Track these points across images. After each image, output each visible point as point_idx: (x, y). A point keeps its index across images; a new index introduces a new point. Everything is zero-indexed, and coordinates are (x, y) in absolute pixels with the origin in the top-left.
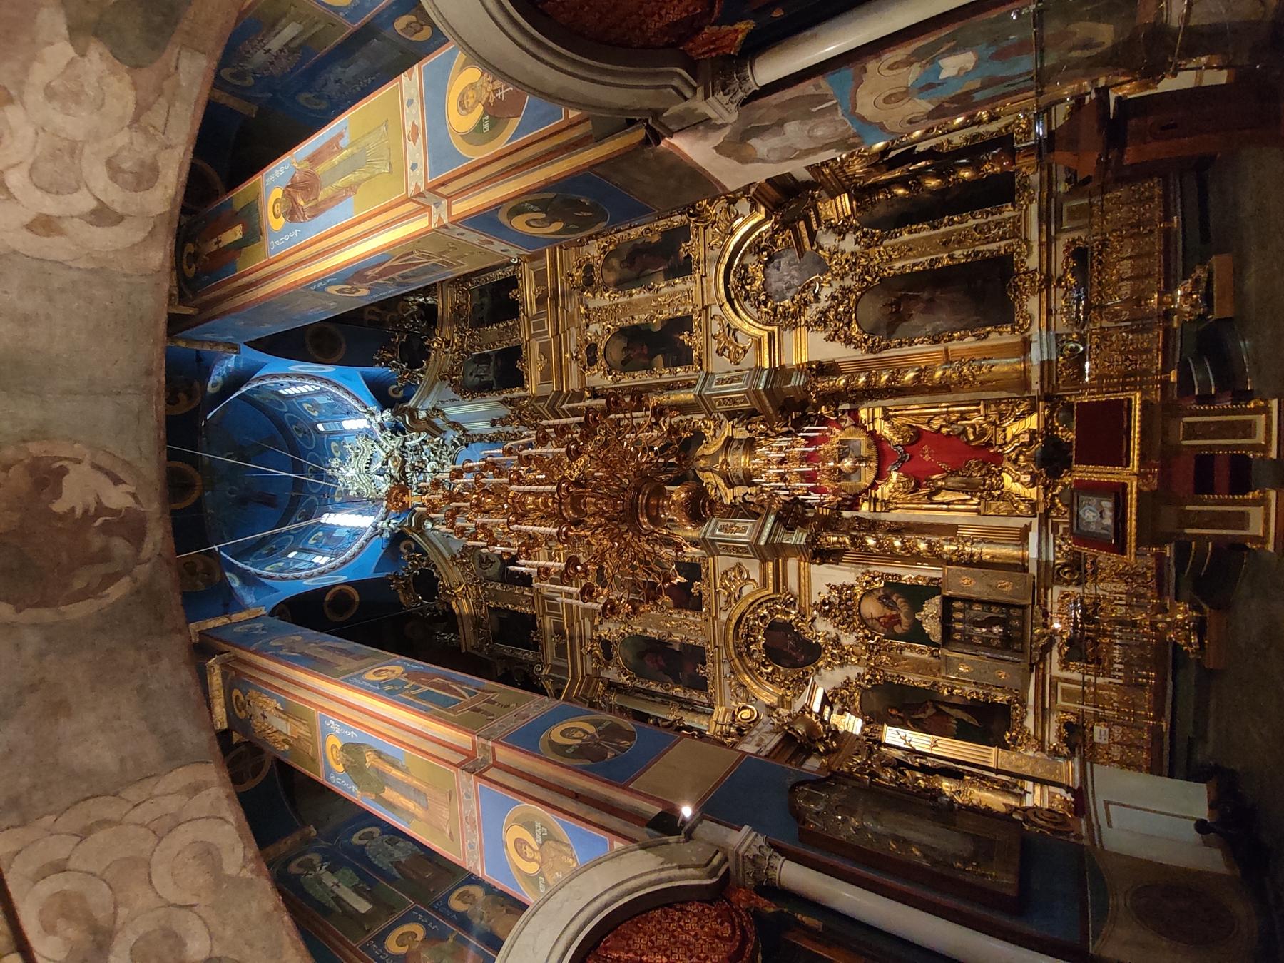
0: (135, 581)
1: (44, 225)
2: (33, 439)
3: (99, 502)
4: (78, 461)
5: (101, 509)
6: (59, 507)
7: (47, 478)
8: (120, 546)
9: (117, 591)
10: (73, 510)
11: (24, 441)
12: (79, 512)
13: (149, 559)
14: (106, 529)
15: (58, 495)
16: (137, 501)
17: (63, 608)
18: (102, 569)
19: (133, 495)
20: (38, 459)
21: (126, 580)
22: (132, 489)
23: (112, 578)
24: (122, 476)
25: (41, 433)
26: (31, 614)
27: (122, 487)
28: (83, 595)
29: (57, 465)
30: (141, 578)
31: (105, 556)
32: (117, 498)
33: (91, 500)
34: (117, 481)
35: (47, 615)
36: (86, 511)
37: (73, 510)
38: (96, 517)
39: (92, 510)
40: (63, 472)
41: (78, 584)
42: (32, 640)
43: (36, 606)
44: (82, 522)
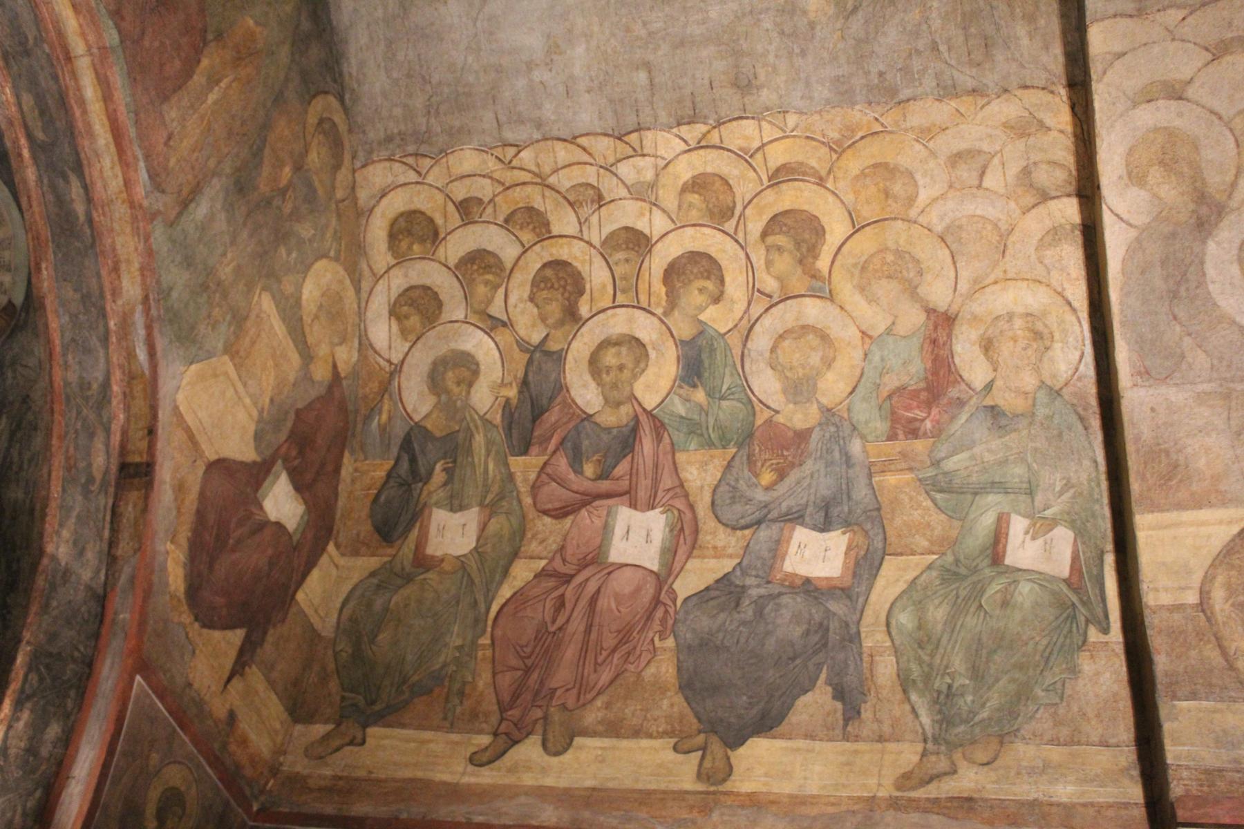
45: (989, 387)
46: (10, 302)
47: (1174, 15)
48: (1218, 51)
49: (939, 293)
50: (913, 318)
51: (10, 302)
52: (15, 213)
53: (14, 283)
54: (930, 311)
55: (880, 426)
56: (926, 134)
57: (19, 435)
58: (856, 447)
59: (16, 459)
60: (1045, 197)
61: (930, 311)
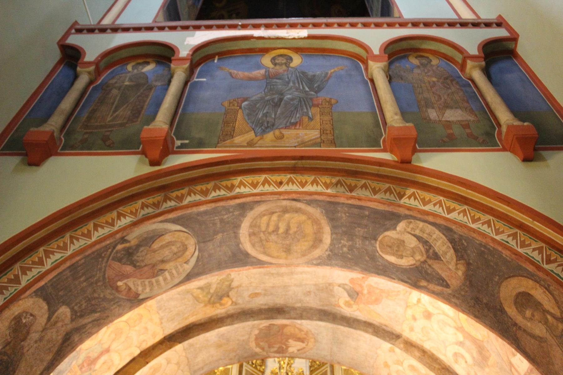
1: (386, 365)
7: (301, 340)
11: (315, 339)
21: (261, 351)
23: (263, 349)
24: (300, 352)
25: (316, 341)
27: (296, 351)
34: (298, 350)
42: (245, 338)
45: (96, 370)
46: (139, 295)
47: (184, 354)
48: (178, 364)
49: (114, 346)
50: (106, 346)
51: (139, 295)
52: (170, 286)
53: (147, 293)
54: (109, 347)
55: (80, 361)
56: (151, 320)
57: (95, 322)
58: (74, 362)
59: (87, 328)
60: (139, 348)
61: (109, 347)
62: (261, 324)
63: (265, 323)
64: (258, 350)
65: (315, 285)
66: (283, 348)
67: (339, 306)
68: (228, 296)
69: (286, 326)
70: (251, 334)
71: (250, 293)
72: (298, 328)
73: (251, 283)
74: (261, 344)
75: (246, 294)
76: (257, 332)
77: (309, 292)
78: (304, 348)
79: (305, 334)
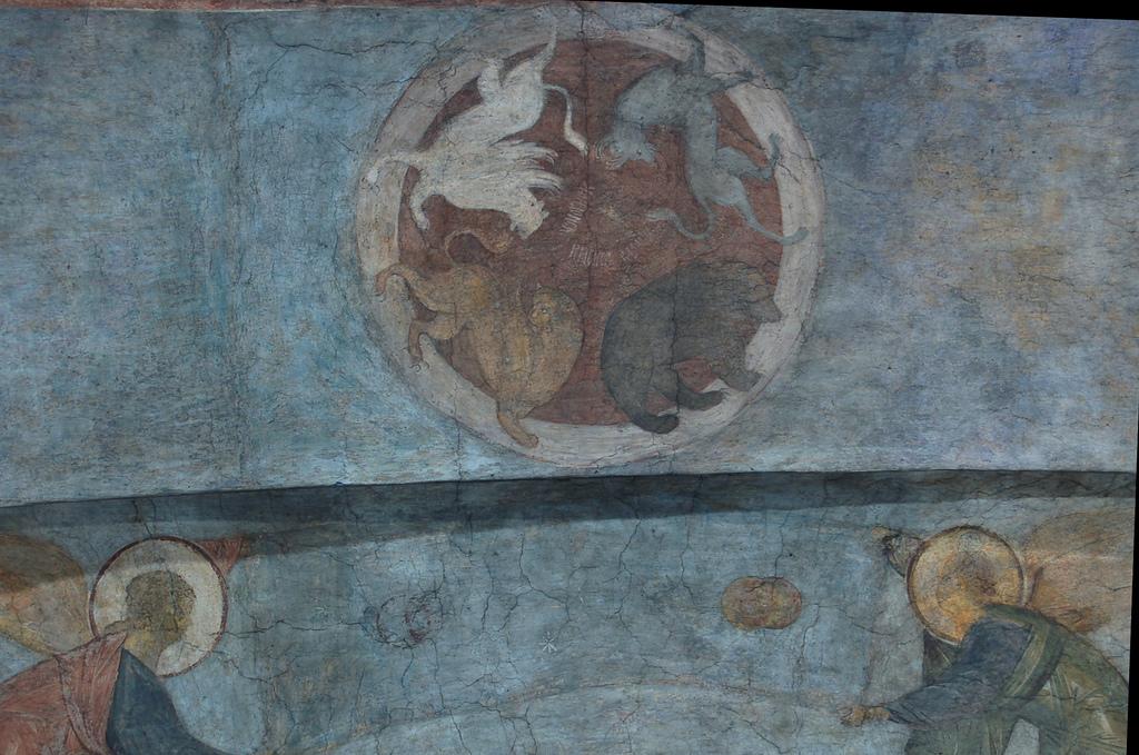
0: (746, 77)
2: (355, 263)
3: (524, 137)
4: (414, 174)
5: (543, 132)
6: (529, 216)
7: (451, 238)
8: (647, 101)
9: (767, 116)
10: (537, 191)
11: (360, 278)
12: (546, 179)
13: (694, 37)
14: (598, 126)
15: (495, 220)
16: (529, 54)
17: (789, 230)
18: (701, 146)
19: (511, 63)
20: (405, 255)
21: (740, 96)
22: (491, 70)
23: (732, 125)
24: (454, 85)
26: (789, 294)
27: (487, 86)
28: (764, 190)
29: (420, 217)
30: (743, 62)
31: (672, 135)
32: (515, 100)
33: (513, 152)
34: (471, 95)
35: (798, 263)
36: (545, 165)
37: (537, 191)
38: (566, 149)
39: (541, 152)
40: (442, 210)
41: (735, 195)
43: (772, 282)
44: (573, 179)
62: (734, 433)
63: (705, 438)
64: (767, 116)
65: (384, 721)
66: (582, 126)
67: (210, 551)
68: (932, 646)
69: (566, 407)
70: (810, 334)
71: (788, 637)
72: (483, 384)
73: (783, 727)
74: (735, 195)
75: (816, 633)
76: (768, 350)
77: (416, 637)
78: (428, 140)
79: (425, 315)
